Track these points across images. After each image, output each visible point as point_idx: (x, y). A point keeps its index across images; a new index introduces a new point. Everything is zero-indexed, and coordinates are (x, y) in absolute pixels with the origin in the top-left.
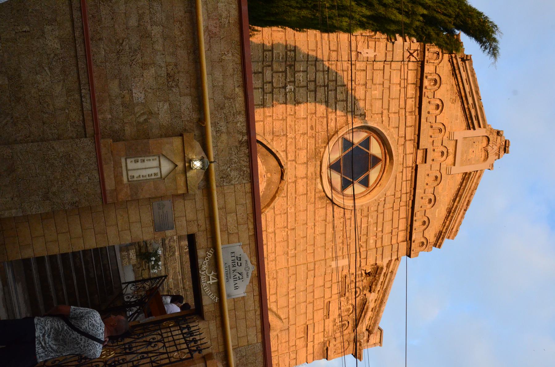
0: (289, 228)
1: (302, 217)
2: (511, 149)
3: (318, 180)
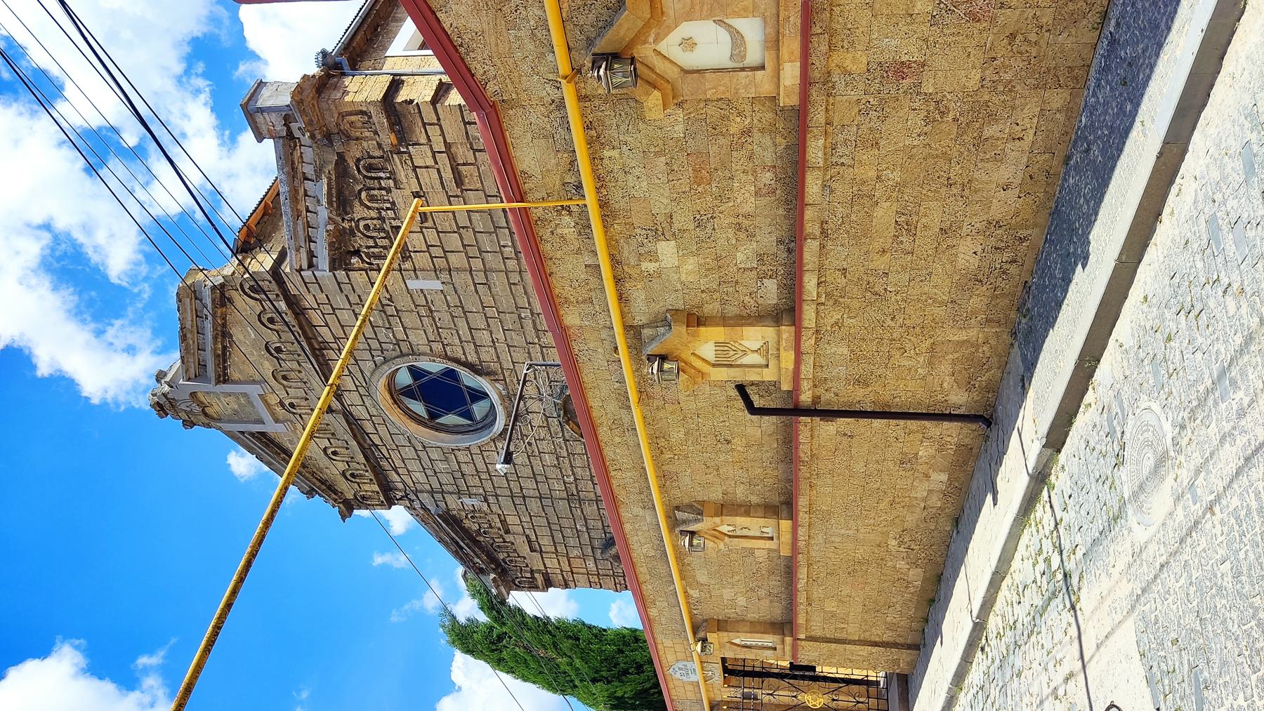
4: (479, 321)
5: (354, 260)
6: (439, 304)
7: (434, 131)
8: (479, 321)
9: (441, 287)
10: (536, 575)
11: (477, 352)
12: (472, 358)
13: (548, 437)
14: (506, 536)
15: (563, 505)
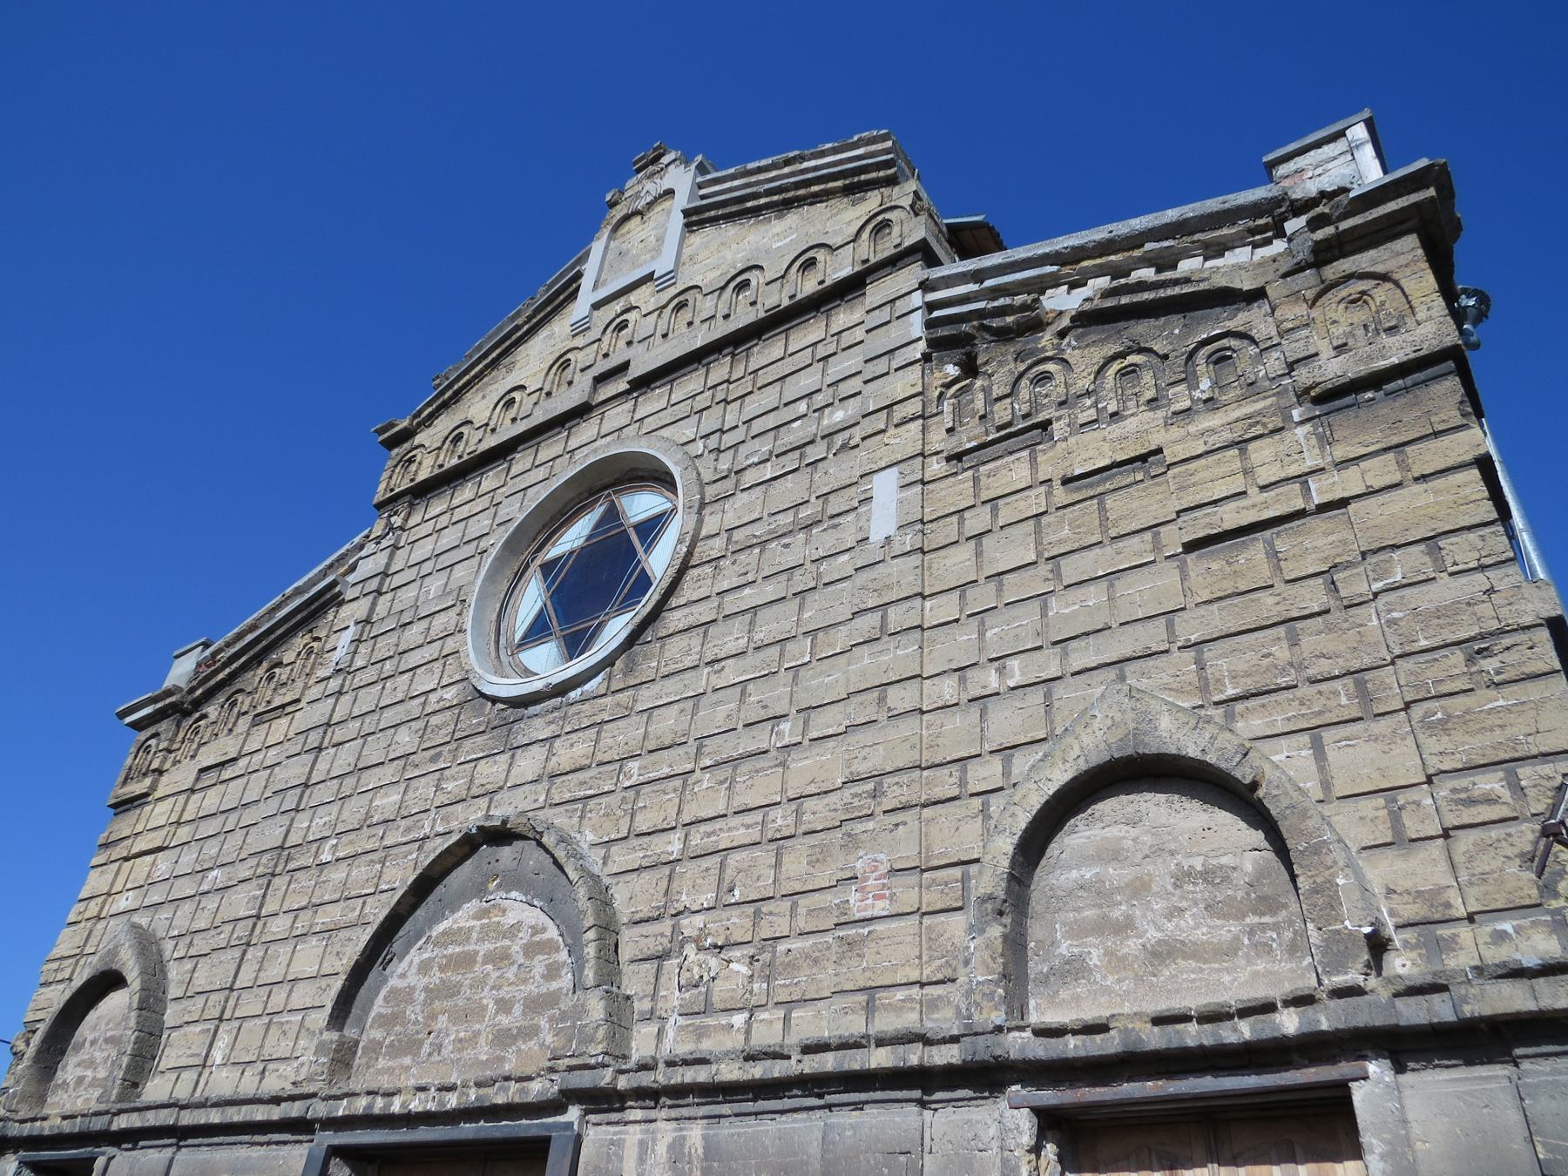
0: (689, 767)
1: (667, 724)
3: (574, 695)
4: (771, 626)
5: (952, 370)
6: (824, 540)
7: (1381, 471)
8: (771, 626)
9: (877, 537)
10: (148, 781)
12: (674, 619)
13: (442, 798)
14: (249, 717)
15: (272, 835)
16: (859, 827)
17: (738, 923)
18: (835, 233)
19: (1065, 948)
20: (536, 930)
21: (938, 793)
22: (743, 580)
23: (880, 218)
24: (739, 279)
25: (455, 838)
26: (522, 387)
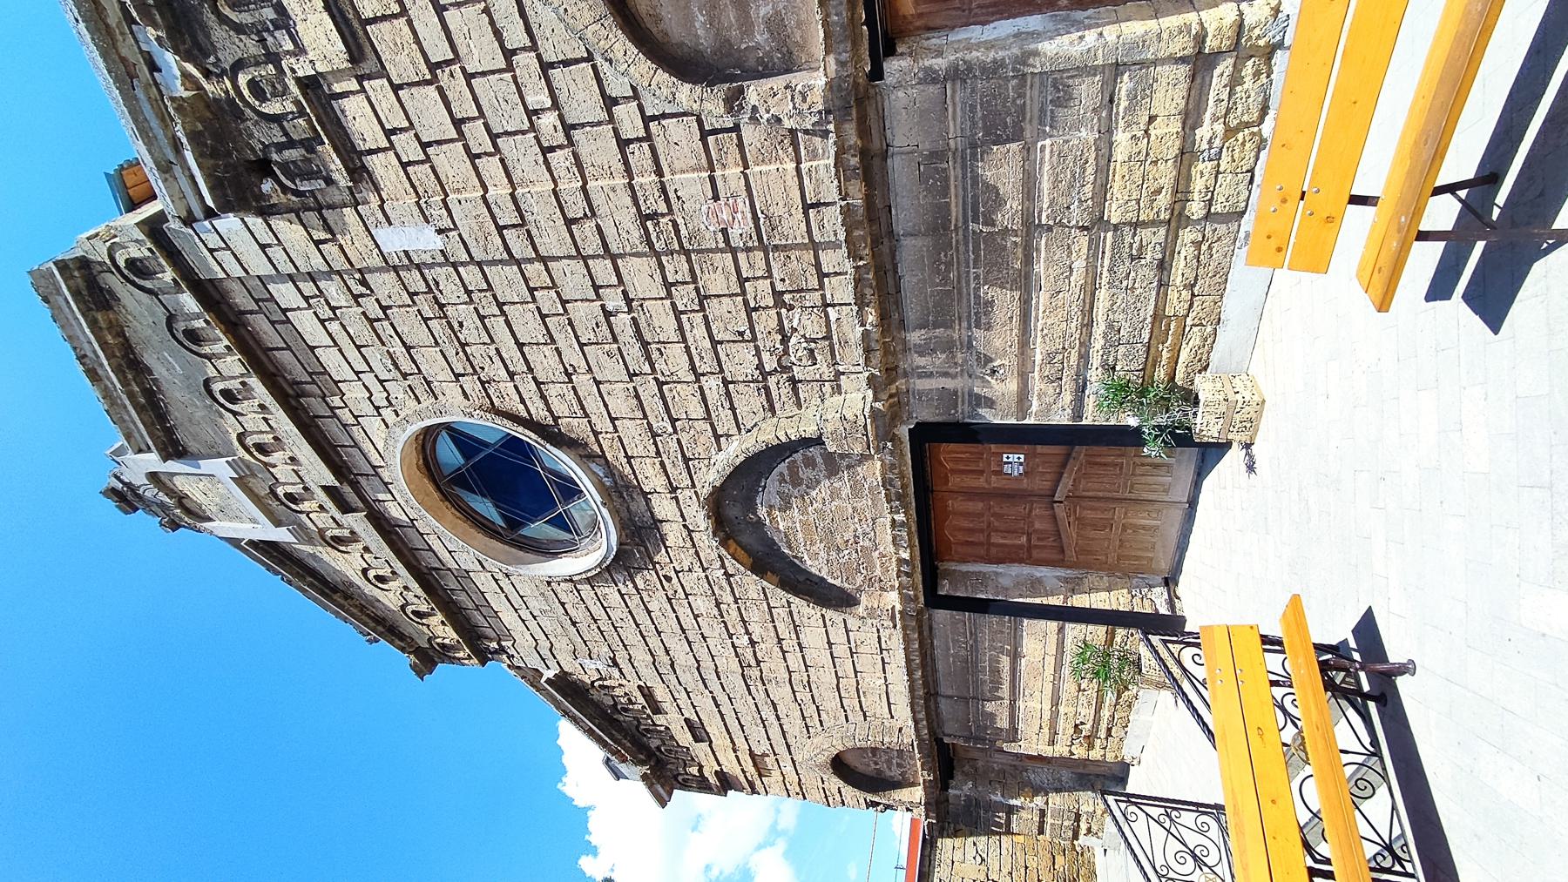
1: (621, 404)
2: (110, 504)
8: (529, 328)
11: (543, 397)
12: (538, 412)
14: (655, 717)
16: (683, 232)
17: (766, 321)
18: (153, 314)
19: (761, 37)
20: (782, 480)
21: (648, 163)
22: (496, 359)
23: (126, 272)
24: (222, 400)
25: (723, 552)
26: (365, 571)
